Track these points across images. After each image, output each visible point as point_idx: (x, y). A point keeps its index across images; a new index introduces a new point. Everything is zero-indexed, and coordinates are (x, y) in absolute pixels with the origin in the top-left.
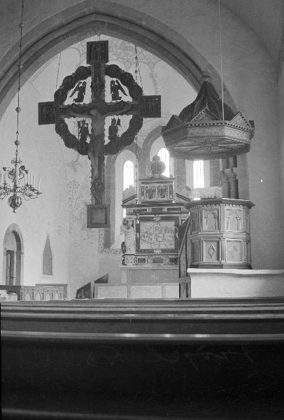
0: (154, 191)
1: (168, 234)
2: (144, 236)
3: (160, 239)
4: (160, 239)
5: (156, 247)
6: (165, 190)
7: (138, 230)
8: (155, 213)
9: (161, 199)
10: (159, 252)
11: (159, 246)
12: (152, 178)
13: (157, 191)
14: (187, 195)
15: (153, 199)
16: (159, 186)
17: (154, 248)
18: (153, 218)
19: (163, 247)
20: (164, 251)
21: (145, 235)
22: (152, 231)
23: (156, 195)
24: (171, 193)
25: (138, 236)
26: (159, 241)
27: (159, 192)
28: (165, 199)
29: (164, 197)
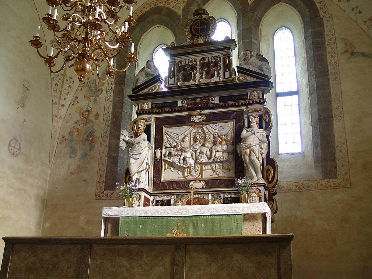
0: (193, 68)
1: (219, 148)
2: (170, 154)
3: (204, 159)
4: (204, 159)
5: (195, 175)
6: (216, 64)
7: (159, 144)
8: (195, 107)
9: (204, 81)
10: (199, 185)
11: (201, 173)
12: (192, 46)
13: (198, 67)
14: (261, 68)
15: (192, 82)
16: (204, 59)
17: (190, 177)
18: (189, 117)
19: (208, 174)
20: (210, 183)
21: (173, 151)
22: (186, 145)
23: (198, 75)
24: (228, 67)
25: (158, 155)
26: (202, 164)
27: (202, 69)
28: (216, 79)
29: (212, 76)
